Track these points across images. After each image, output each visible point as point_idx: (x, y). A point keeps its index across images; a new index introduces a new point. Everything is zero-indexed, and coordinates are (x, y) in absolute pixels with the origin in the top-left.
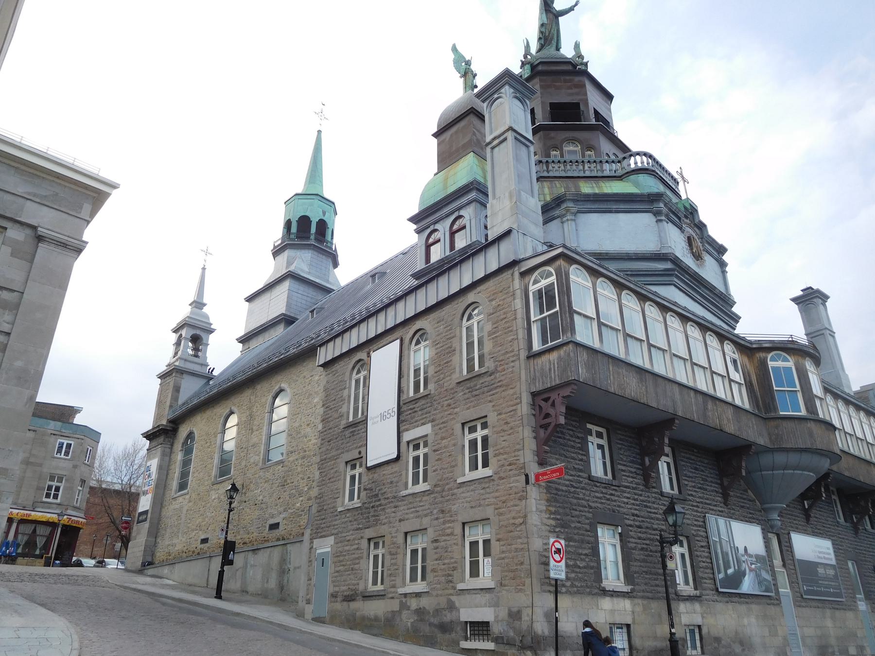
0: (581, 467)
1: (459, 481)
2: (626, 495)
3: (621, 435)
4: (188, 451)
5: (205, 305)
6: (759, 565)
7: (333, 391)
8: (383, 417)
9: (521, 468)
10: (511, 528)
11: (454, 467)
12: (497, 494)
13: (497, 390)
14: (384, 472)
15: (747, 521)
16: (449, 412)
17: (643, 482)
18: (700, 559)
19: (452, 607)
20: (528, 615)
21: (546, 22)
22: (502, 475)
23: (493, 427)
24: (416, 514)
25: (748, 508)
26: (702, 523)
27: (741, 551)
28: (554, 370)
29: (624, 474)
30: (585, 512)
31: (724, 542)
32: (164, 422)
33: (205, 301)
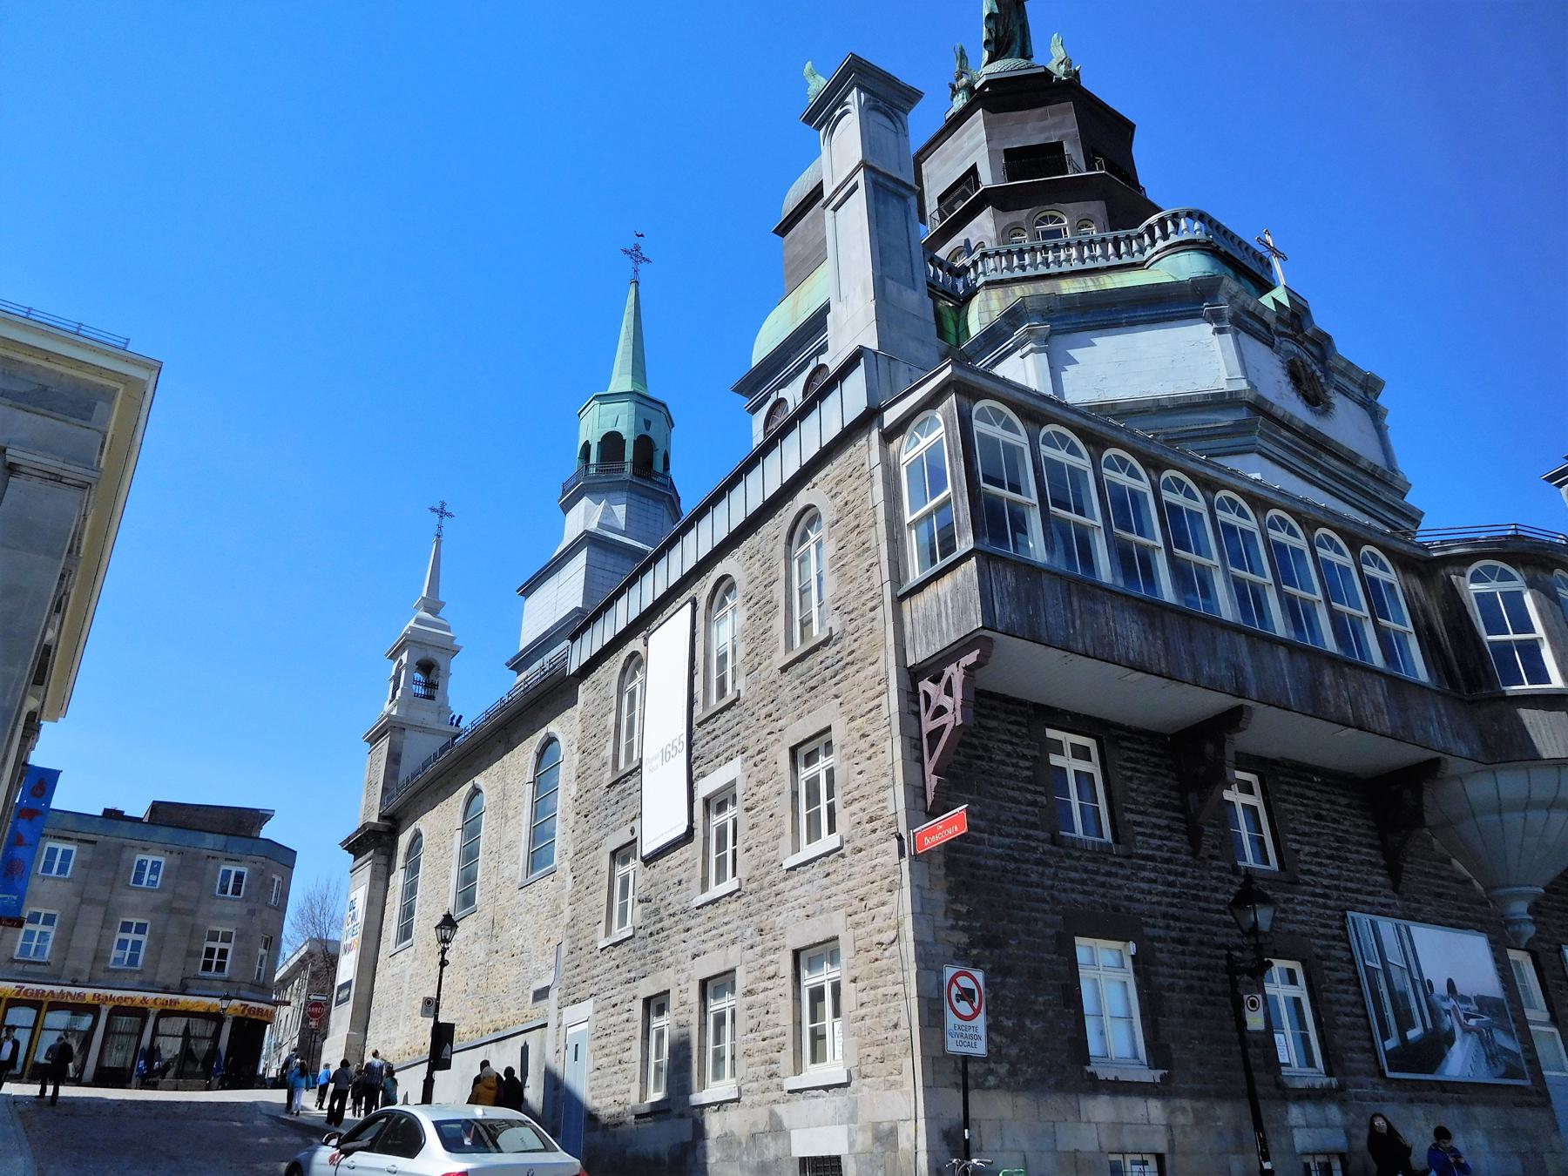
0: (1033, 819)
2: (1146, 874)
3: (1129, 749)
4: (413, 869)
5: (443, 604)
6: (1486, 1018)
8: (666, 756)
10: (876, 953)
12: (851, 884)
13: (847, 672)
14: (669, 864)
15: (1452, 926)
16: (768, 730)
17: (1189, 847)
18: (1336, 1008)
19: (777, 1129)
20: (908, 1138)
21: (996, 11)
22: (859, 843)
23: (843, 747)
25: (1455, 898)
26: (1338, 932)
27: (1440, 988)
28: (947, 613)
29: (1142, 830)
30: (1045, 912)
31: (1396, 975)
32: (375, 819)
33: (441, 599)
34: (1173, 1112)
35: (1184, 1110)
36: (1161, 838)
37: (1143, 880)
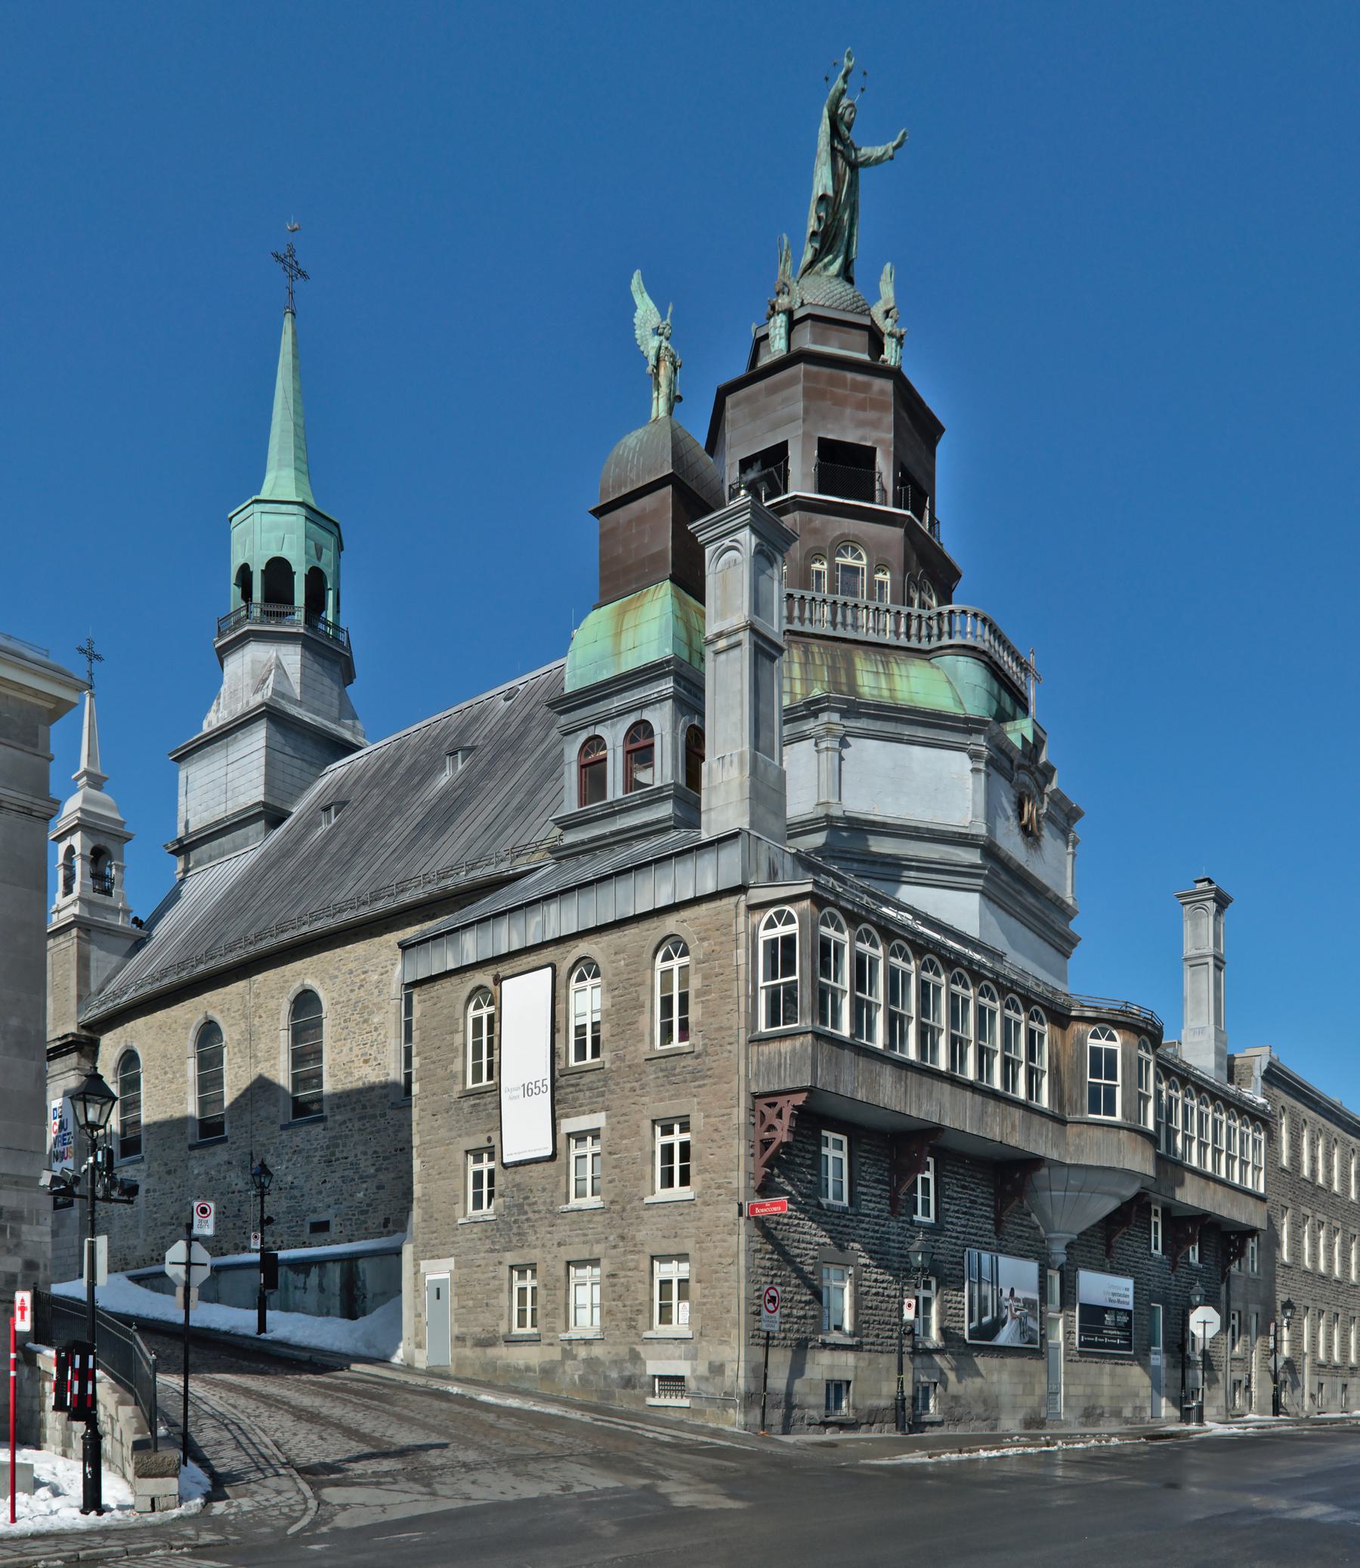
1: (648, 1200)
7: (434, 1033)
9: (733, 1194)
11: (639, 1180)
12: (700, 1224)
19: (635, 1357)
20: (732, 1370)
24: (583, 1239)
35: (864, 1359)
37: (862, 1229)
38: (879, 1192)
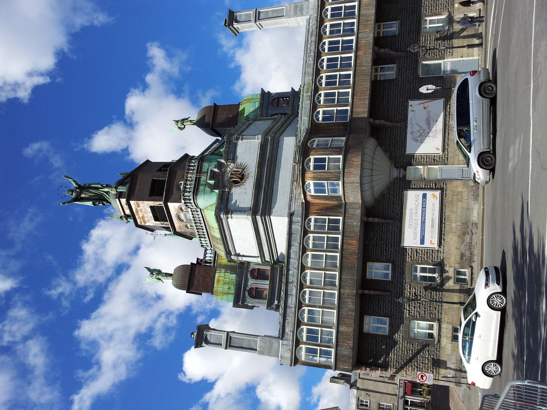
2: (395, 312)
25: (394, 196)
34: (444, 321)
35: (444, 317)
36: (386, 305)
38: (382, 301)
